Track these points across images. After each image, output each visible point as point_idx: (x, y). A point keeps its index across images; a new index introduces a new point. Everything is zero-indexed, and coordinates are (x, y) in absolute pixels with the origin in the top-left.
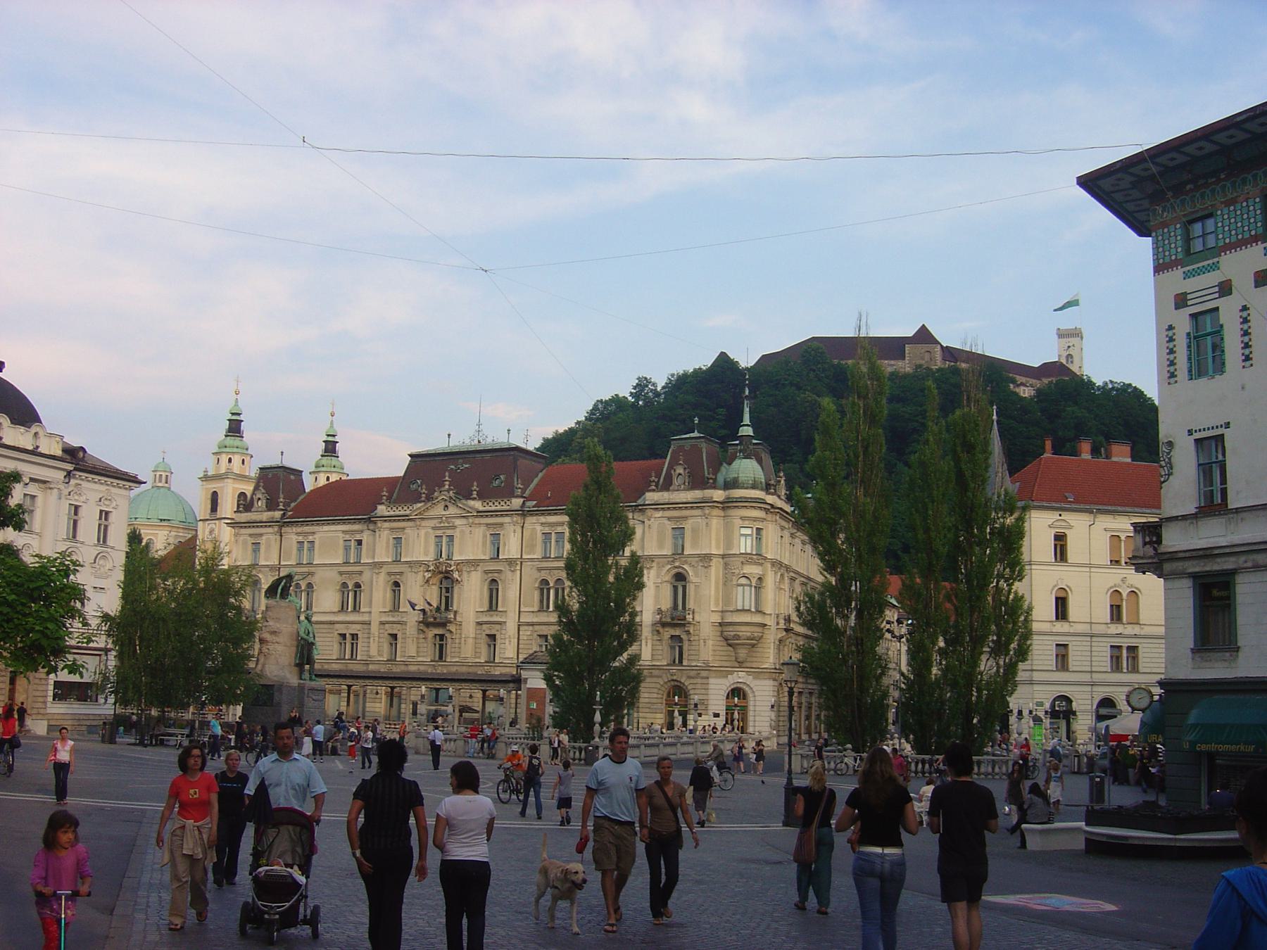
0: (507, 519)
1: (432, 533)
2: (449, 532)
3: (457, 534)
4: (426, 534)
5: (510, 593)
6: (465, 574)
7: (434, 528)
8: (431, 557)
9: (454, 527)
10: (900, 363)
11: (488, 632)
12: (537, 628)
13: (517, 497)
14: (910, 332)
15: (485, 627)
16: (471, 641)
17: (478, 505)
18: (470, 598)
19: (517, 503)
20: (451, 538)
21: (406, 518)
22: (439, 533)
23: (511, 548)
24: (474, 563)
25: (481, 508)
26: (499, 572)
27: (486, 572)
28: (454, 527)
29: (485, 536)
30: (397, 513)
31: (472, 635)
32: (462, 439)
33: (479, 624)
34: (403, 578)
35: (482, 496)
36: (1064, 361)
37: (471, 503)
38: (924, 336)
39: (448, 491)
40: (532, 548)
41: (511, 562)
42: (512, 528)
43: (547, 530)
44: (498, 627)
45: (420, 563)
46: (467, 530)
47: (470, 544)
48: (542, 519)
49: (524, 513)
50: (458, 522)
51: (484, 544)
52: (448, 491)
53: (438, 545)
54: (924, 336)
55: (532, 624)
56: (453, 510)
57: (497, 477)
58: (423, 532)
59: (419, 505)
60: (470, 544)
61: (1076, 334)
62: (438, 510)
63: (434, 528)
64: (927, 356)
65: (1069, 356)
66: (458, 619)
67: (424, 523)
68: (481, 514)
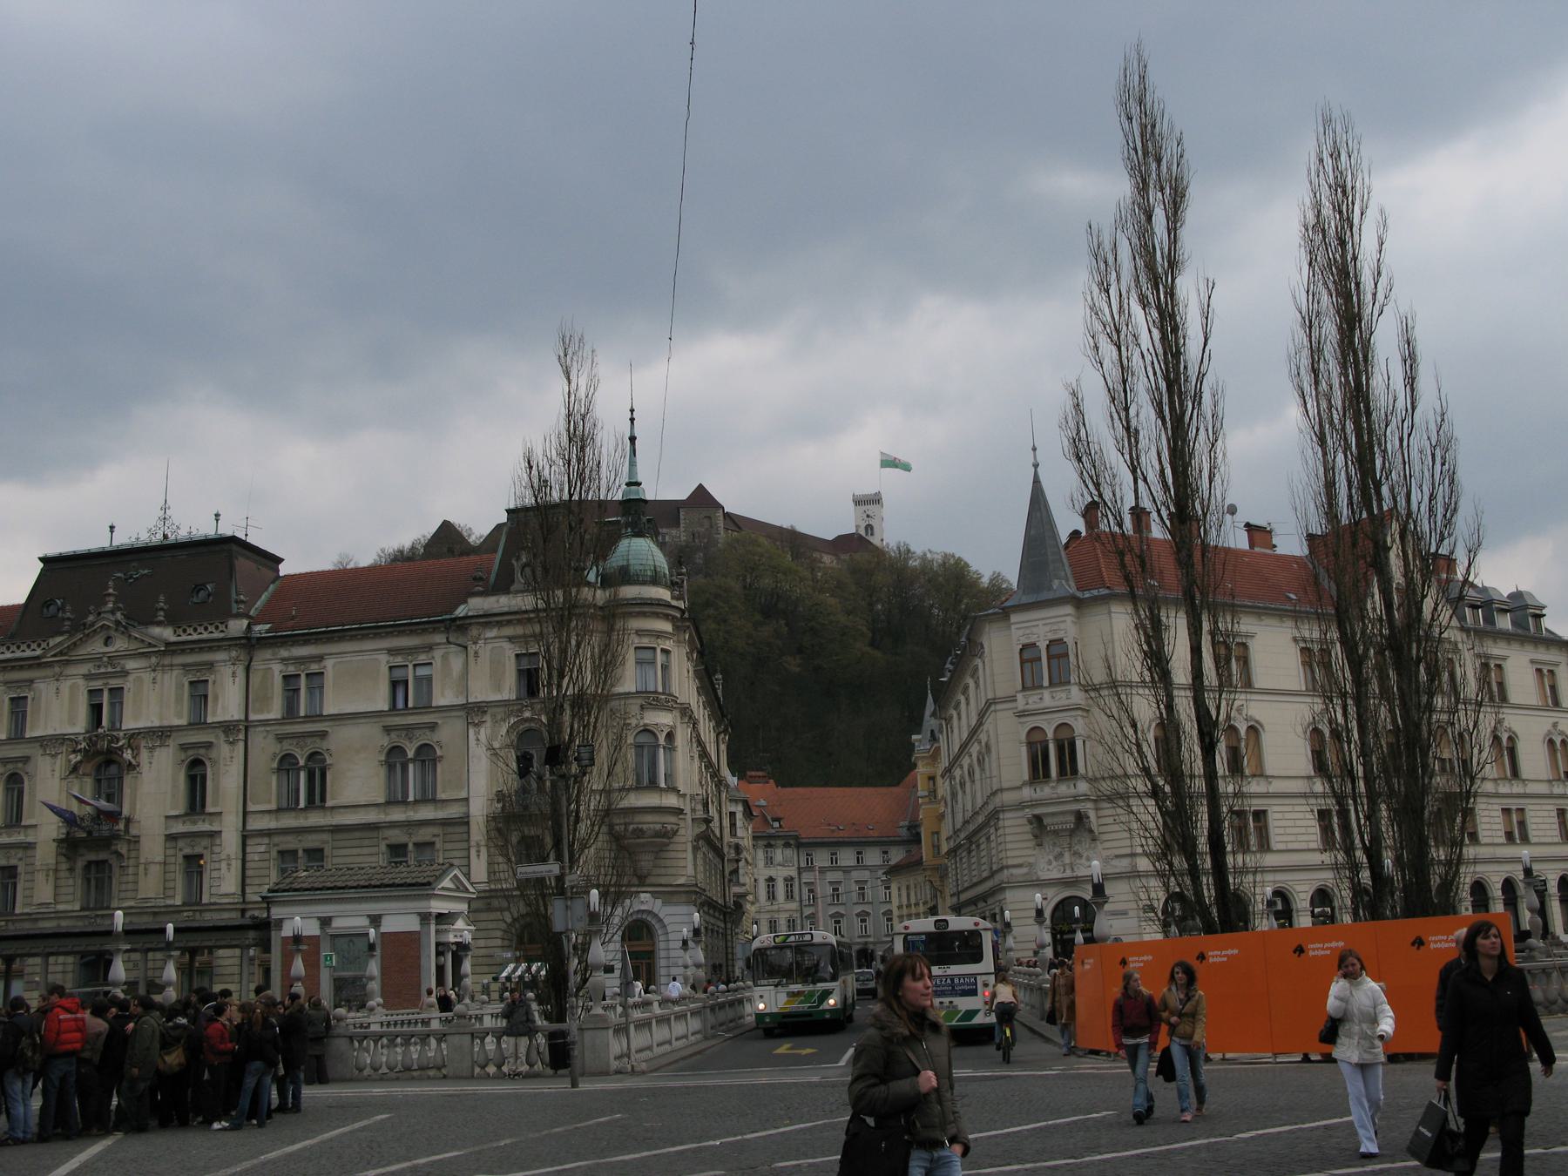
0: (220, 656)
1: (83, 687)
2: (114, 683)
3: (129, 684)
4: (73, 688)
5: (226, 781)
6: (144, 754)
7: (88, 677)
8: (80, 726)
9: (125, 673)
10: (674, 532)
11: (188, 851)
12: (276, 839)
13: (238, 616)
14: (683, 495)
15: (181, 844)
16: (155, 870)
17: (168, 633)
18: (153, 793)
19: (237, 626)
20: (117, 692)
21: (36, 663)
22: (97, 684)
23: (228, 703)
24: (161, 734)
25: (173, 639)
26: (209, 745)
27: (184, 748)
28: (125, 673)
29: (180, 686)
30: (18, 654)
31: (160, 858)
32: (136, 530)
33: (171, 838)
34: (29, 768)
35: (173, 620)
36: (863, 533)
37: (156, 630)
38: (701, 497)
39: (113, 612)
40: (265, 701)
41: (228, 728)
42: (228, 670)
43: (291, 670)
44: (205, 842)
45: (61, 739)
46: (147, 677)
47: (152, 701)
48: (284, 653)
49: (249, 644)
50: (131, 665)
51: (179, 700)
52: (113, 612)
53: (96, 710)
54: (701, 497)
55: (268, 833)
56: (120, 644)
57: (199, 588)
58: (66, 686)
59: (59, 639)
60: (152, 701)
61: (876, 500)
62: (96, 647)
63: (88, 677)
64: (706, 522)
65: (869, 528)
66: (133, 831)
67: (72, 670)
68: (172, 649)
